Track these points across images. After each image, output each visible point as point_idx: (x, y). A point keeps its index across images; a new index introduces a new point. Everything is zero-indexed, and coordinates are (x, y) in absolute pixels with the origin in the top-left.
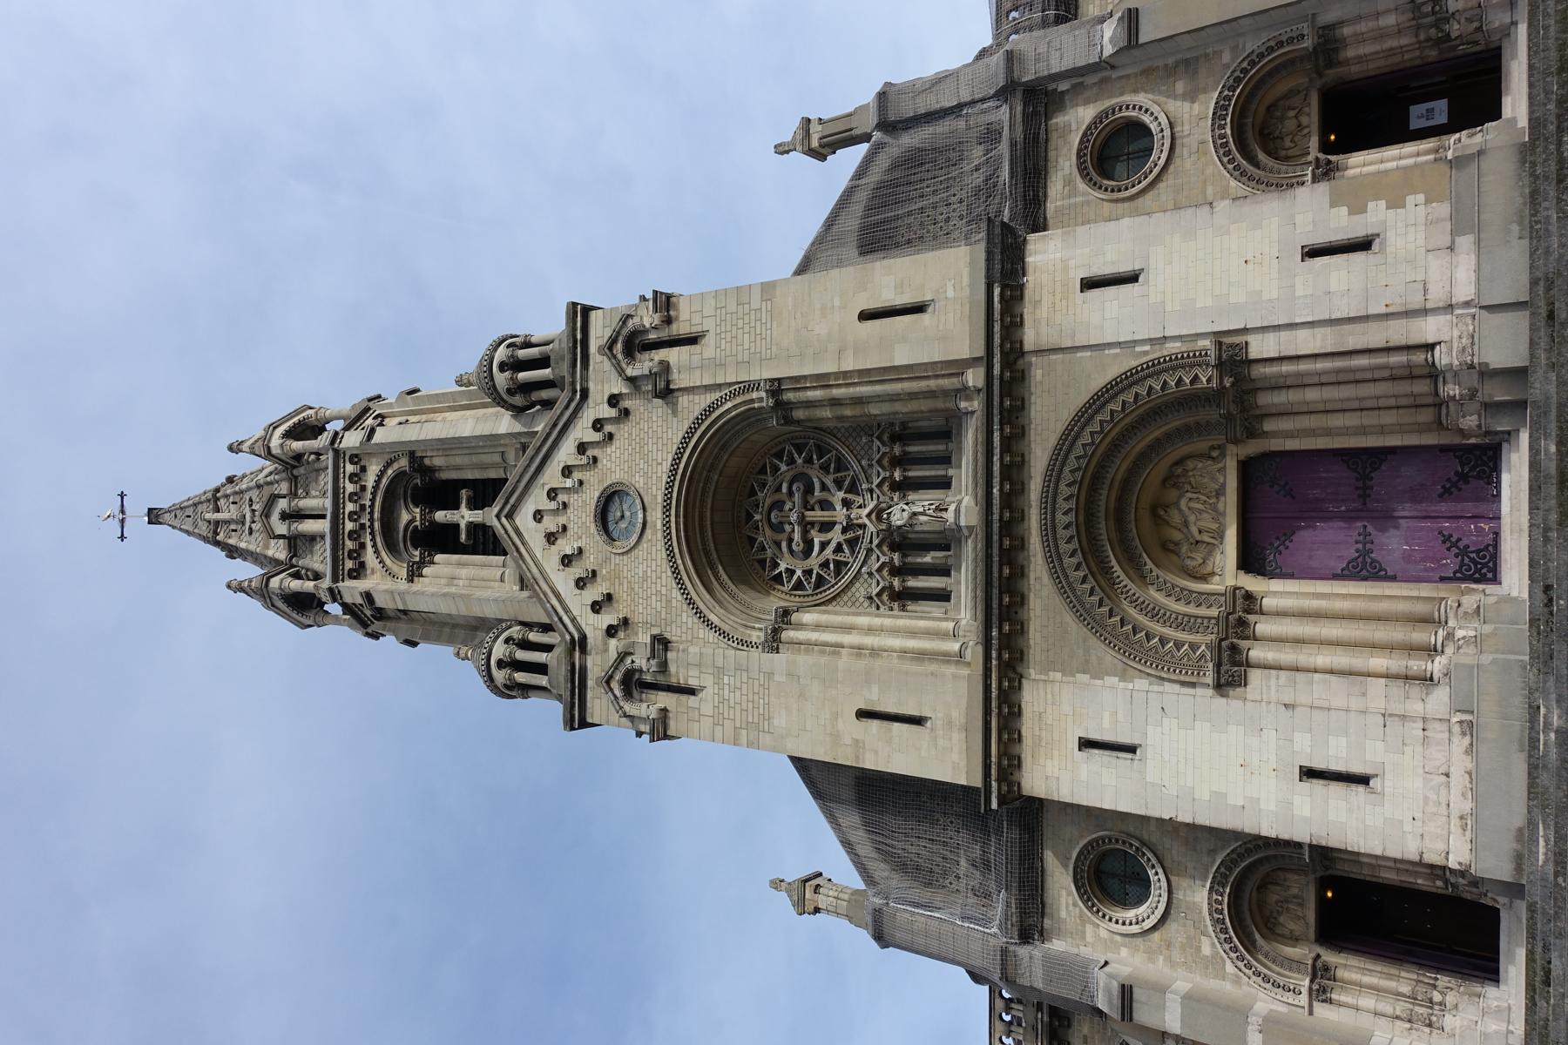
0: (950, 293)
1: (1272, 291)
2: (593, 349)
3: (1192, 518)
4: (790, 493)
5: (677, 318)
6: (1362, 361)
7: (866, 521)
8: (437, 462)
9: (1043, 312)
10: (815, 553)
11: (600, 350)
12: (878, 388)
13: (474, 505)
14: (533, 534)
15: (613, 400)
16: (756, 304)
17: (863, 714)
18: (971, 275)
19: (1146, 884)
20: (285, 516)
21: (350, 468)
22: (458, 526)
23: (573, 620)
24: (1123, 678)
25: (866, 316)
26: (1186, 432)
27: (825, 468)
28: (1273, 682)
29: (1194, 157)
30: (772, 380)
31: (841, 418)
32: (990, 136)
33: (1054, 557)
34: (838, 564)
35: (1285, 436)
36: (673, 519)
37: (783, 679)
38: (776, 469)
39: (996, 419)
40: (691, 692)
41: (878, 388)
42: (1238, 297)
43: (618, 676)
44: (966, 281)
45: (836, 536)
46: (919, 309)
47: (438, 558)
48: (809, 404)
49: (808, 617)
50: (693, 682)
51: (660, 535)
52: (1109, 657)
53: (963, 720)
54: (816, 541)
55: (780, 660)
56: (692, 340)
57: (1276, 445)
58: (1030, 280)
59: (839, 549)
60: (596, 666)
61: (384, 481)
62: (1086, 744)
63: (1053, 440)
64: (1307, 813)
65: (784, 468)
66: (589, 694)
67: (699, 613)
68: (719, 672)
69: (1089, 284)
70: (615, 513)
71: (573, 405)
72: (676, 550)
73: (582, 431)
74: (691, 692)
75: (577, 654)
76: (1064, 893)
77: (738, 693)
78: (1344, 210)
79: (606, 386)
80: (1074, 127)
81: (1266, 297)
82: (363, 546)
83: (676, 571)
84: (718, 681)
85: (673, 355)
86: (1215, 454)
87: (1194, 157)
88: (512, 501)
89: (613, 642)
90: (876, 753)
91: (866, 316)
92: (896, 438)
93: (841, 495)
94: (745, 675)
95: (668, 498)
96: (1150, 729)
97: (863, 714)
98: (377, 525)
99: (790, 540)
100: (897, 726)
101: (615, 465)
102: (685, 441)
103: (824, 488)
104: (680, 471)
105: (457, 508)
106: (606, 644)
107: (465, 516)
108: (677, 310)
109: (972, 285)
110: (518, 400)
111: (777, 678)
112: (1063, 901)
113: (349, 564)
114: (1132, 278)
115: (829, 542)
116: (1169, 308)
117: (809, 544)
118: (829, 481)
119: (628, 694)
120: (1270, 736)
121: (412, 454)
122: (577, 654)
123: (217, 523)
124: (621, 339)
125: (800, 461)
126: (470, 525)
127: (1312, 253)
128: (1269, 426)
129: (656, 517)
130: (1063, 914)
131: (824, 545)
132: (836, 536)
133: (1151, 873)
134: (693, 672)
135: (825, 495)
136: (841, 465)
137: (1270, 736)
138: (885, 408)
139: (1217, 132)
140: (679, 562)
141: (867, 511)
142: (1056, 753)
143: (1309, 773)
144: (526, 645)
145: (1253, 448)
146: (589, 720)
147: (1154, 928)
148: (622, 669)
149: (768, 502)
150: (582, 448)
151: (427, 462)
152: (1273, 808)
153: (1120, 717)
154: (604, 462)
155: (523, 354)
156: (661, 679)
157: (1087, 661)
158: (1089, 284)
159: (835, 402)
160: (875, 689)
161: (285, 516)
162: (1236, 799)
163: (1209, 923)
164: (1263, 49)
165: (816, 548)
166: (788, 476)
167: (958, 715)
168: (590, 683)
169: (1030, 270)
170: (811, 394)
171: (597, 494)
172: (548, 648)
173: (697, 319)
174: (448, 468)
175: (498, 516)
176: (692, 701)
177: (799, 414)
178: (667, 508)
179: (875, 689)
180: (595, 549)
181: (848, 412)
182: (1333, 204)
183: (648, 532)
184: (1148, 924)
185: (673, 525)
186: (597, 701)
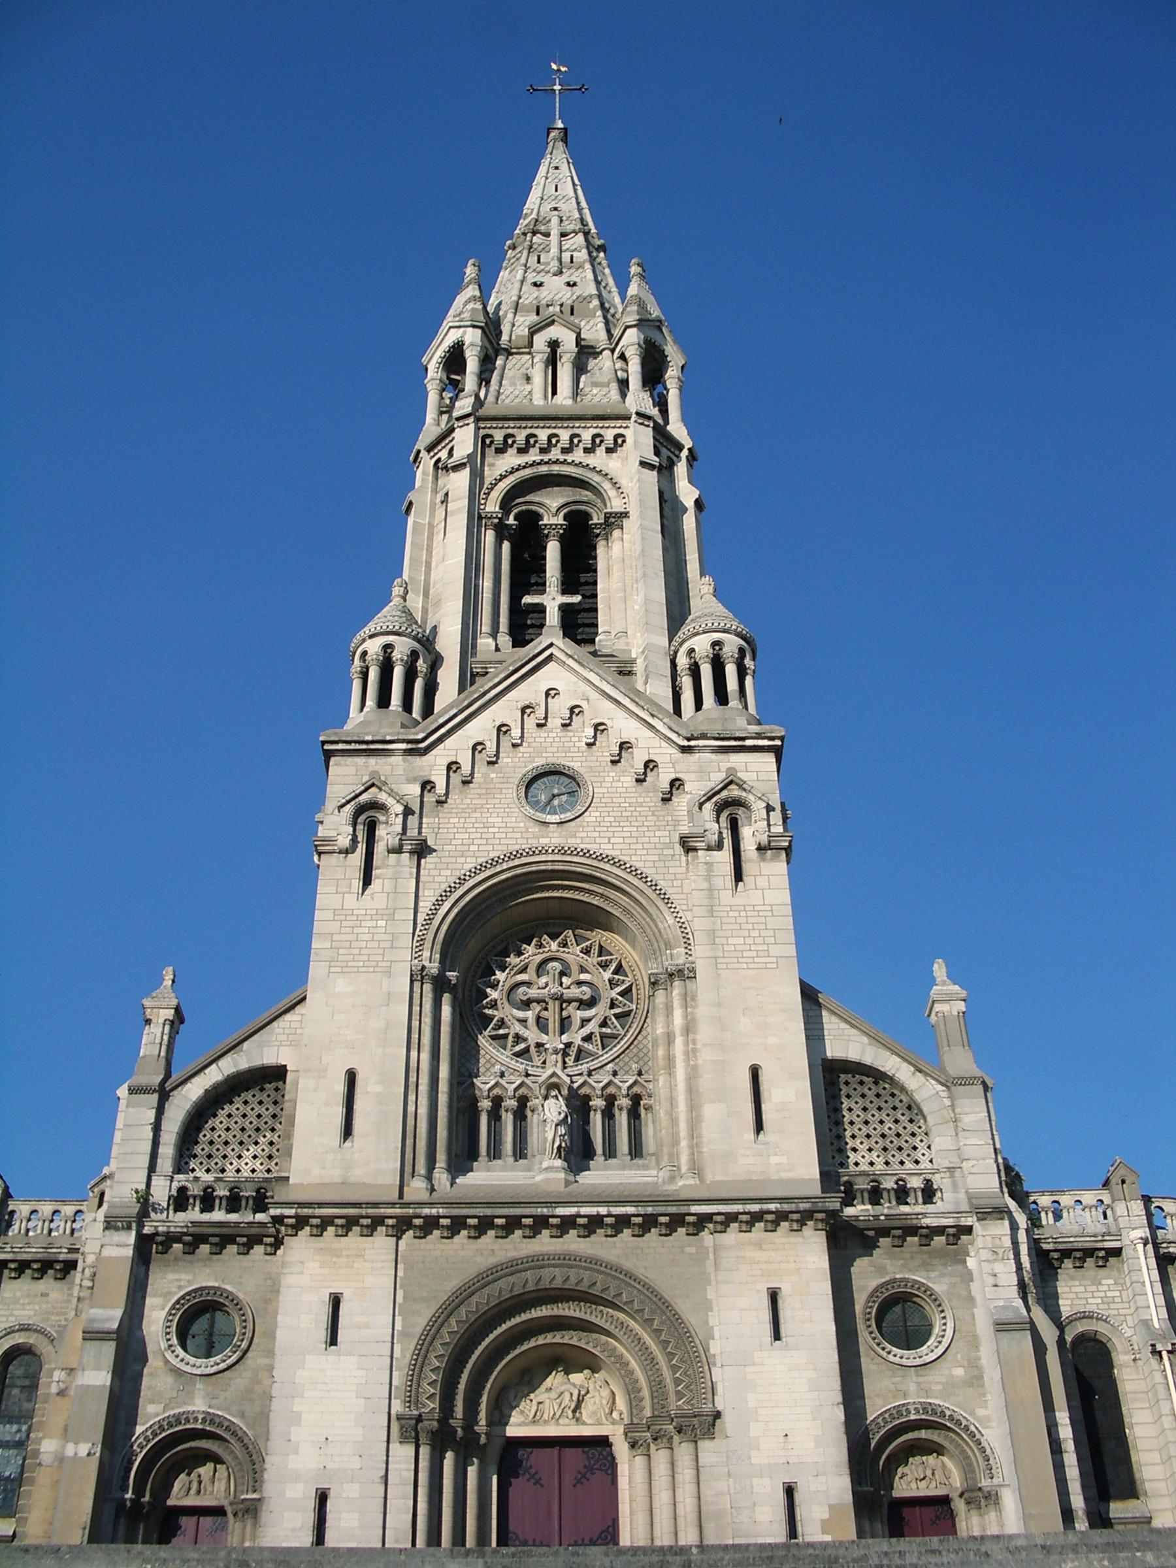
0: (774, 1160)
1: (758, 1459)
3: (554, 1395)
4: (580, 983)
5: (763, 859)
7: (549, 1072)
8: (616, 547)
9: (751, 1253)
10: (515, 1011)
11: (731, 771)
13: (565, 609)
14: (531, 690)
15: (676, 784)
16: (776, 950)
17: (351, 1077)
18: (792, 1181)
19: (208, 1355)
20: (554, 345)
21: (609, 435)
22: (543, 592)
23: (440, 740)
24: (405, 1334)
25: (755, 1072)
27: (604, 1024)
28: (404, 1466)
29: (892, 1387)
30: (693, 970)
31: (655, 1043)
32: (929, 1193)
33: (514, 1267)
34: (506, 1036)
36: (550, 858)
37: (385, 989)
38: (604, 966)
39: (650, 1210)
40: (367, 881)
41: (681, 1086)
42: (755, 1430)
43: (383, 797)
44: (785, 1175)
45: (533, 1035)
46: (759, 1126)
50: (376, 884)
51: (534, 842)
52: (420, 1322)
53: (353, 1180)
54: (530, 1015)
55: (403, 984)
56: (738, 876)
57: (623, 1469)
59: (518, 1038)
61: (595, 479)
62: (336, 1302)
63: (627, 1264)
64: (290, 1494)
65: (607, 975)
66: (360, 760)
67: (451, 890)
68: (390, 915)
69: (774, 1296)
70: (556, 777)
71: (674, 736)
72: (517, 862)
73: (647, 745)
74: (367, 881)
75: (403, 746)
76: (189, 1277)
77: (368, 937)
78: (826, 1516)
79: (693, 776)
80: (932, 1274)
81: (754, 1453)
82: (522, 451)
83: (495, 862)
84: (380, 915)
86: (615, 1415)
87: (892, 1387)
88: (570, 662)
89: (417, 790)
90: (316, 1090)
91: (755, 1072)
92: (636, 1099)
93: (578, 1041)
94: (388, 945)
95: (574, 852)
96: (354, 1359)
97: (351, 1078)
98: (544, 469)
99: (528, 984)
100: (339, 1111)
101: (610, 786)
102: (633, 871)
103: (585, 1022)
104: (601, 865)
105: (564, 592)
106: (415, 780)
107: (552, 600)
108: (772, 860)
109: (781, 1181)
110: (683, 661)
111: (385, 981)
112: (183, 1276)
113: (499, 436)
114: (777, 1336)
115: (526, 1027)
116: (749, 1369)
117: (526, 1004)
119: (360, 810)
120: (356, 1463)
121: (625, 515)
122: (403, 746)
123: (547, 235)
124: (744, 794)
125: (613, 994)
126: (540, 609)
127: (790, 1491)
128: (640, 1461)
129: (553, 838)
130: (171, 1276)
131: (523, 1021)
132: (533, 1035)
133: (217, 1358)
134: (388, 885)
135: (576, 1022)
136: (606, 1040)
137: (356, 1463)
139: (911, 1408)
140: (505, 866)
141: (560, 1073)
142: (326, 1271)
143: (322, 1498)
144: (410, 675)
145: (621, 1448)
146: (333, 760)
147: (167, 1361)
148: (389, 801)
149: (570, 958)
150: (624, 746)
151: (616, 533)
152: (291, 1465)
153: (363, 1331)
154: (612, 773)
155: (731, 671)
156: (380, 848)
157: (415, 1300)
158: (774, 1296)
159: (670, 1039)
160: (379, 1089)
161: (554, 345)
162: (296, 1434)
163: (177, 1411)
164: (984, 1444)
165: (520, 1014)
166: (595, 981)
167: (358, 1174)
168: (372, 761)
169: (796, 1239)
171: (576, 765)
172: (407, 705)
173: (762, 882)
174: (609, 559)
175: (551, 645)
176: (357, 884)
177: (660, 996)
178: (562, 851)
179: (379, 1089)
180: (518, 764)
181: (661, 1052)
182: (831, 1507)
183: (535, 829)
184: (168, 1355)
185: (543, 858)
186: (352, 770)
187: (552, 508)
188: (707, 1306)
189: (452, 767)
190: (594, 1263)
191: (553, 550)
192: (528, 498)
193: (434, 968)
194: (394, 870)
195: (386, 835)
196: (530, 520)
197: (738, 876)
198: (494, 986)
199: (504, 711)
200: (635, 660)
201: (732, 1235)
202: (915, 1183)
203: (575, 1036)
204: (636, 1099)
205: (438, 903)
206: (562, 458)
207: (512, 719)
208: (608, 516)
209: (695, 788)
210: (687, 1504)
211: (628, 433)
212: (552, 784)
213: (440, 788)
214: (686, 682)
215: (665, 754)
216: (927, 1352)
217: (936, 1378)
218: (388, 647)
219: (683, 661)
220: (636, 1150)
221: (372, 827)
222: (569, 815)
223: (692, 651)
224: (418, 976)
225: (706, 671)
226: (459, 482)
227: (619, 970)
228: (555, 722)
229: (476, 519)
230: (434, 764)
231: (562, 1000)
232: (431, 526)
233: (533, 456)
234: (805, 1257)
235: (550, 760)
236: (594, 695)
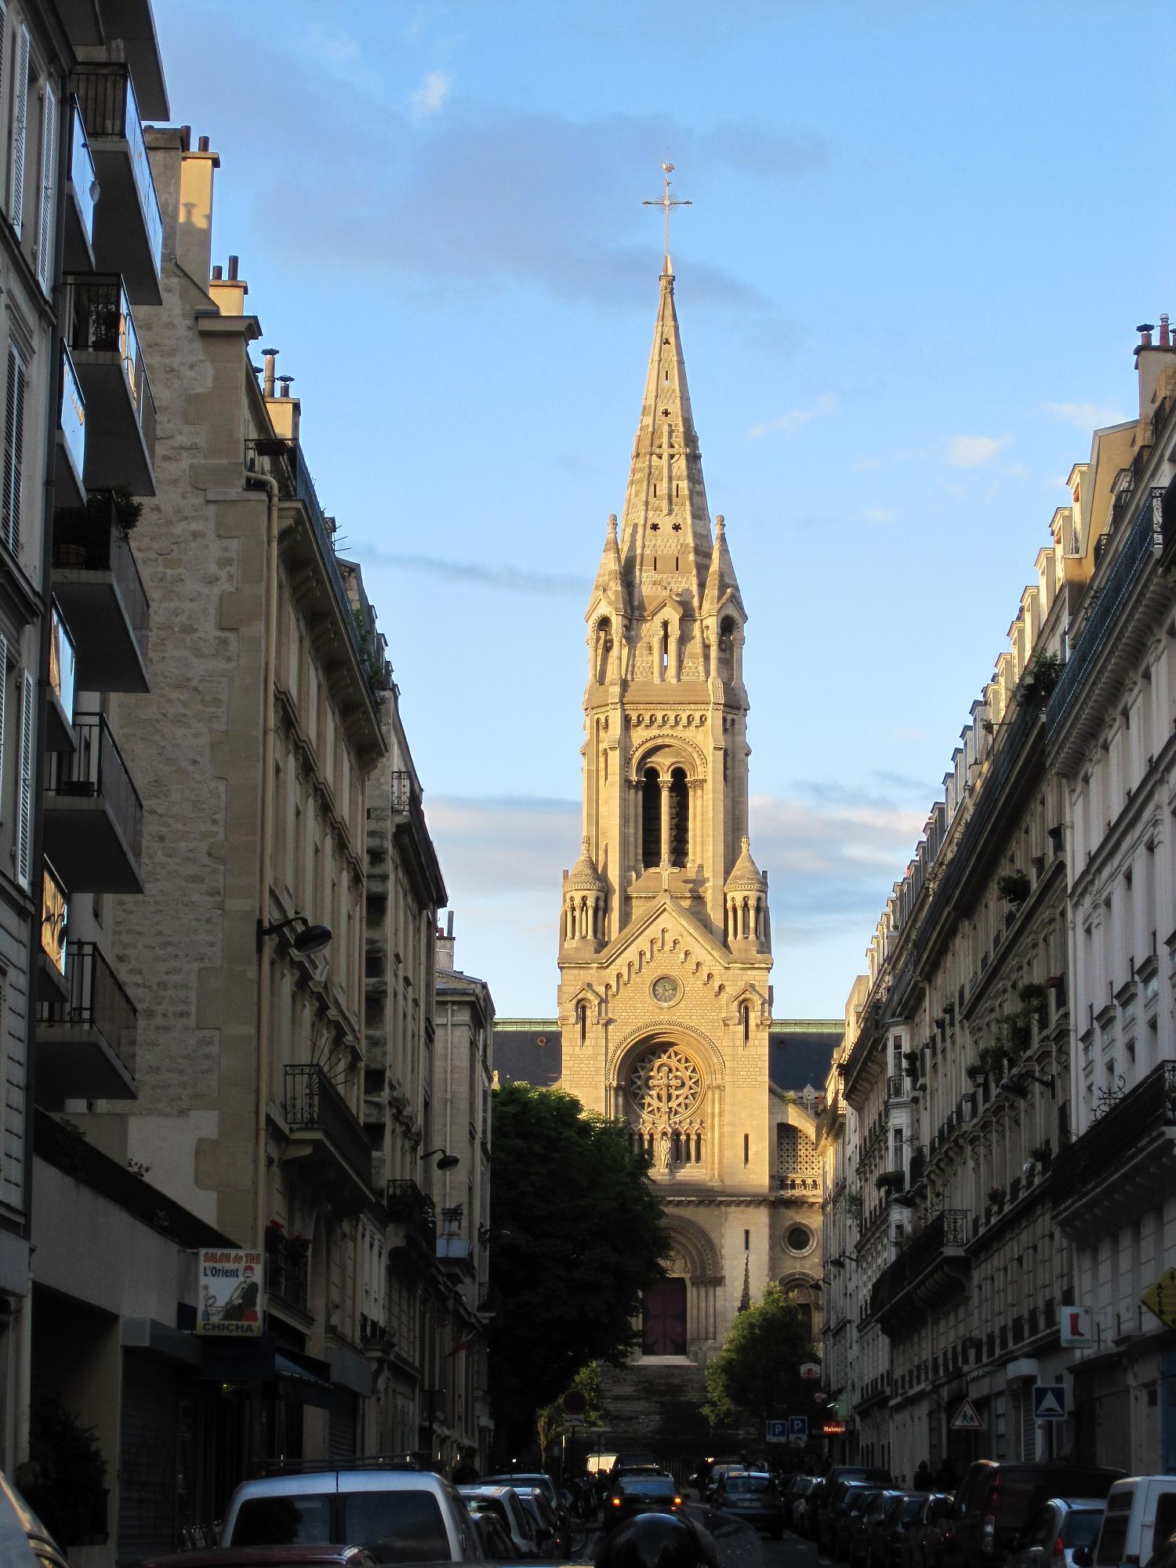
2: (749, 972)
4: (676, 1077)
6: (712, 1320)
8: (699, 802)
9: (739, 1215)
12: (716, 1141)
16: (759, 1078)
20: (665, 624)
25: (746, 1137)
26: (693, 1263)
35: (691, 1293)
40: (584, 1037)
41: (716, 1141)
45: (655, 1103)
47: (640, 794)
48: (713, 1103)
49: (621, 1100)
50: (588, 1042)
51: (657, 1019)
56: (747, 1037)
58: (751, 1209)
60: (591, 975)
63: (693, 1218)
66: (576, 971)
68: (595, 1058)
69: (747, 1232)
74: (584, 1037)
83: (639, 1029)
85: (742, 1028)
91: (746, 1137)
92: (699, 1136)
101: (692, 985)
118: (681, 1099)
119: (579, 1001)
129: (665, 1017)
138: (709, 1140)
145: (688, 1283)
151: (699, 792)
156: (588, 1021)
158: (747, 1232)
161: (665, 624)
170: (717, 1106)
176: (579, 1041)
180: (650, 973)
187: (663, 763)
188: (722, 1236)
189: (619, 976)
190: (680, 1218)
191: (665, 795)
192: (653, 759)
193: (615, 1084)
194: (594, 1031)
195: (591, 1014)
196: (652, 774)
197: (747, 1037)
198: (639, 1078)
199: (643, 943)
200: (706, 880)
201: (732, 1209)
202: (809, 1181)
203: (673, 1104)
204: (699, 1136)
205: (615, 1052)
206: (670, 732)
207: (647, 947)
208: (695, 781)
209: (731, 990)
210: (711, 1309)
211: (709, 715)
212: (664, 986)
213: (614, 989)
214: (731, 914)
215: (717, 970)
216: (806, 1252)
217: (807, 1263)
218: (584, 899)
219: (729, 904)
220: (698, 1158)
221: (584, 1008)
222: (672, 1003)
223: (733, 899)
224: (608, 1088)
225: (740, 913)
226: (615, 758)
227: (694, 1071)
228: (667, 948)
229: (626, 783)
230: (610, 975)
231: (669, 1086)
232: (597, 771)
233: (654, 732)
234: (759, 1220)
235: (666, 972)
236: (685, 933)
